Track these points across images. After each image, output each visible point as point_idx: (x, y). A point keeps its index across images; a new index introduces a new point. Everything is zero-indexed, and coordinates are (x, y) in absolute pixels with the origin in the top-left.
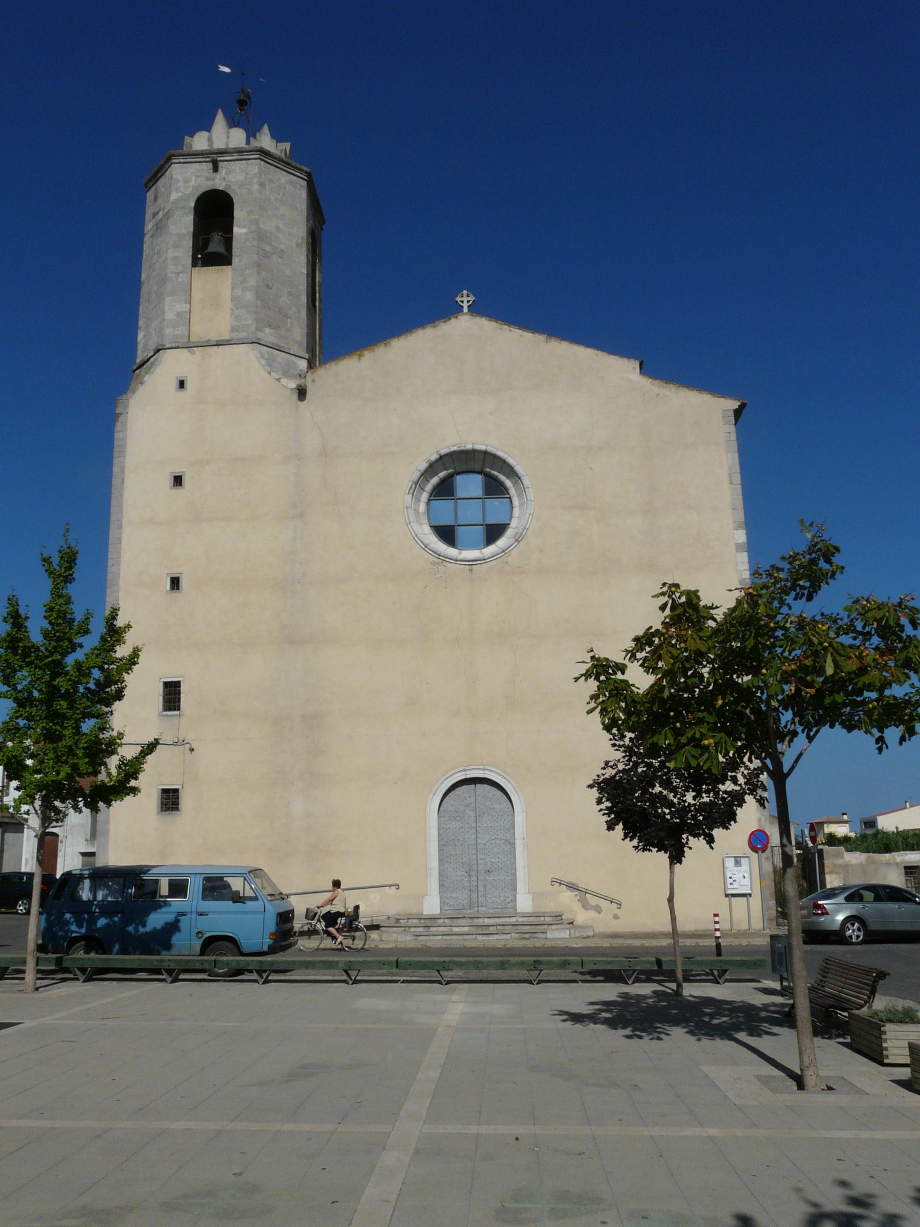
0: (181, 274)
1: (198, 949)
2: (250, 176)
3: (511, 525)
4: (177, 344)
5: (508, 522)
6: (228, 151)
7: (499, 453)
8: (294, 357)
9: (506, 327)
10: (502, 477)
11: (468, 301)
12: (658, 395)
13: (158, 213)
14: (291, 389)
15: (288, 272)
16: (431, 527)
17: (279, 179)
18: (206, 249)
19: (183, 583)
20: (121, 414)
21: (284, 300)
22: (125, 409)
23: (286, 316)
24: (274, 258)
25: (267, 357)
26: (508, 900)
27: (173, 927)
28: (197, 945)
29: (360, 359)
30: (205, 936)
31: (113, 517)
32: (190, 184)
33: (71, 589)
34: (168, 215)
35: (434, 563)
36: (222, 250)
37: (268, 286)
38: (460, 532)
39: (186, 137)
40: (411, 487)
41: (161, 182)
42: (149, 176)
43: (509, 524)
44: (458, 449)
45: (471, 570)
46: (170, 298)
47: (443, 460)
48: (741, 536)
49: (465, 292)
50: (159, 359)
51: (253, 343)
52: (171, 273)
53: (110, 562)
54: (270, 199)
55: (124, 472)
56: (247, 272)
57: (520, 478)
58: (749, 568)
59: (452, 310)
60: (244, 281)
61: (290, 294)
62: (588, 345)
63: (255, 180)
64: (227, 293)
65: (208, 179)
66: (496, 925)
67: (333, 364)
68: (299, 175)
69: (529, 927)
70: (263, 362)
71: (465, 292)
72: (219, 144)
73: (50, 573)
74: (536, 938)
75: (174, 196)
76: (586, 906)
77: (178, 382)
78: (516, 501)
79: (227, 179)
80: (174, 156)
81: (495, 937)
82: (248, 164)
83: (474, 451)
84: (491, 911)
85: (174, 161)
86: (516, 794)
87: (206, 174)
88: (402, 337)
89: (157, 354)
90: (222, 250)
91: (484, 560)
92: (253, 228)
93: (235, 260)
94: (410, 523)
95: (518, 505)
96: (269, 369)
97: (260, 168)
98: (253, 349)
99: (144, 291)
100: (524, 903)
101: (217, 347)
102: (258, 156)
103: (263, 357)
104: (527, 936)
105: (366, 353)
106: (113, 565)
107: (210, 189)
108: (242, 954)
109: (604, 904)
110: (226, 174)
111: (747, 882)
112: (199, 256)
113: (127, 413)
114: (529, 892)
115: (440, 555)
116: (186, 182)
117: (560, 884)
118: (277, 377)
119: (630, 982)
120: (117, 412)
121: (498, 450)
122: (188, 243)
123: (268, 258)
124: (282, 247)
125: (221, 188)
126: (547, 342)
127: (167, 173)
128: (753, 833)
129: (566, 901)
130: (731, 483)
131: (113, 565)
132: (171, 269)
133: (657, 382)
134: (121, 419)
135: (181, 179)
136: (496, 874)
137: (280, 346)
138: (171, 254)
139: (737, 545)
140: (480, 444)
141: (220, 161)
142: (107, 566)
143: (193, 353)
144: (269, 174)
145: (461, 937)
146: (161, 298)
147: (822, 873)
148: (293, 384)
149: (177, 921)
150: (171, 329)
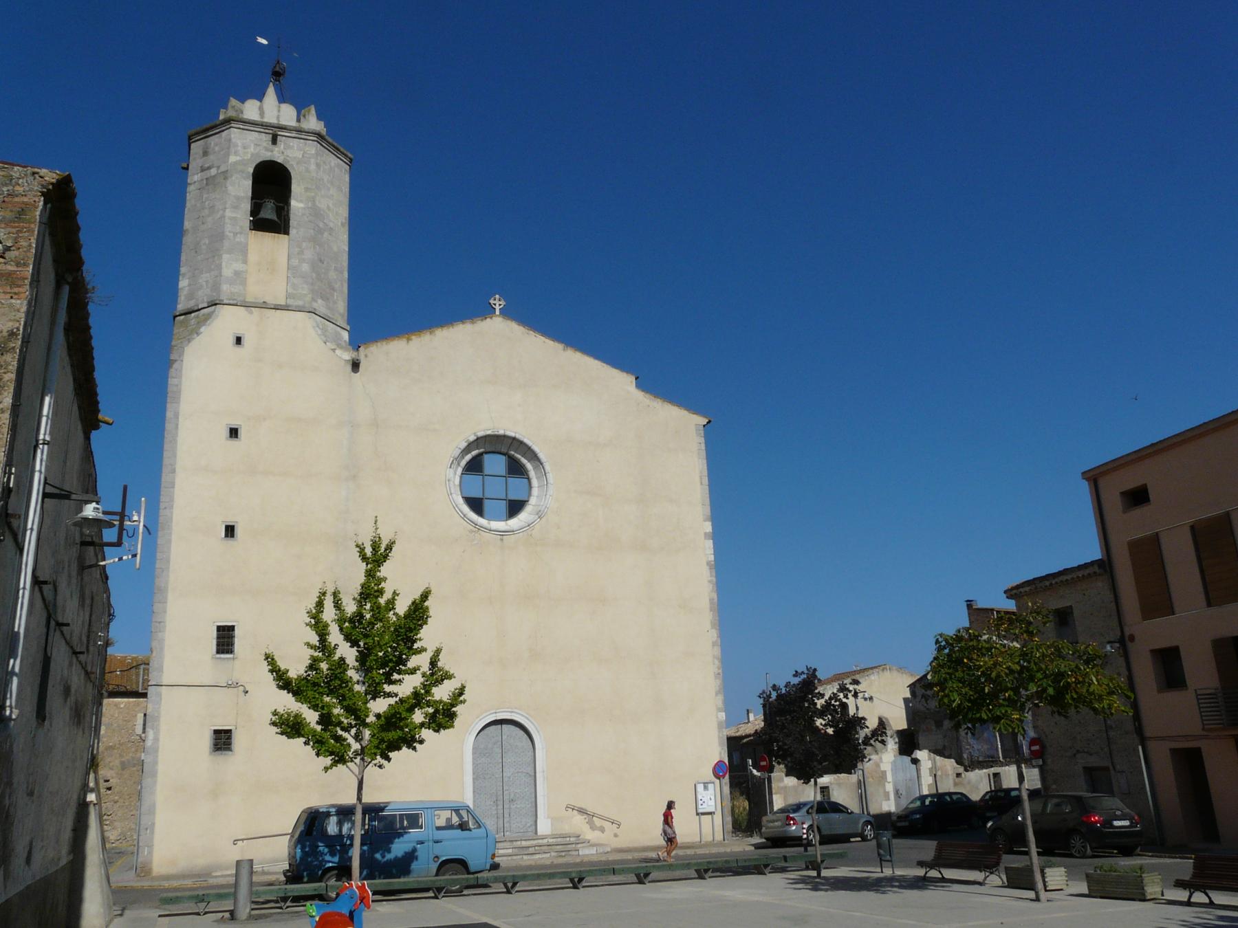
0: (239, 235)
1: (434, 871)
3: (530, 502)
4: (235, 302)
5: (526, 499)
6: (288, 128)
7: (526, 441)
8: (339, 328)
9: (531, 332)
10: (524, 461)
11: (500, 305)
12: (649, 406)
13: (209, 168)
14: (345, 360)
15: (335, 249)
16: (463, 497)
18: (258, 214)
19: (238, 531)
20: (176, 361)
21: (333, 275)
22: (180, 357)
23: (333, 289)
24: (326, 234)
25: (321, 327)
26: (529, 825)
27: (411, 856)
28: (434, 867)
29: (408, 342)
30: (440, 861)
31: (166, 461)
32: (249, 150)
33: (384, 571)
34: (225, 175)
35: (471, 531)
37: (321, 261)
38: (487, 505)
39: (231, 98)
40: (453, 461)
41: (213, 141)
42: (199, 129)
43: (528, 501)
44: (492, 433)
45: (502, 540)
46: (228, 256)
47: (479, 441)
48: (708, 527)
49: (497, 296)
50: (216, 312)
51: (309, 312)
52: (230, 232)
53: (162, 506)
54: (323, 180)
55: (178, 418)
56: (304, 245)
57: (542, 464)
58: (714, 552)
59: (486, 311)
60: (301, 253)
61: (336, 269)
62: (596, 357)
64: (283, 260)
65: (267, 149)
66: (535, 846)
67: (384, 343)
68: (345, 160)
69: (561, 847)
70: (320, 332)
71: (497, 296)
73: (364, 558)
74: (570, 855)
75: (233, 159)
76: (593, 827)
77: (235, 338)
78: (535, 482)
80: (233, 120)
81: (537, 856)
82: (306, 144)
83: (505, 436)
84: (514, 835)
85: (232, 125)
86: (537, 734)
87: (265, 144)
88: (446, 328)
89: (213, 307)
90: (274, 217)
91: (513, 531)
92: (310, 205)
93: (293, 231)
94: (451, 494)
95: (537, 486)
96: (325, 339)
98: (310, 318)
99: (188, 240)
100: (544, 827)
101: (274, 310)
102: (315, 139)
103: (318, 326)
104: (563, 854)
105: (413, 337)
106: (165, 508)
107: (269, 159)
108: (469, 873)
109: (607, 825)
110: (284, 148)
111: (712, 803)
113: (182, 361)
114: (548, 818)
115: (476, 525)
116: (245, 148)
117: (573, 809)
118: (333, 348)
119: (766, 871)
120: (172, 358)
121: (525, 437)
122: (247, 206)
123: (322, 234)
124: (331, 225)
125: (279, 161)
126: (564, 350)
127: (224, 134)
128: (717, 764)
129: (578, 824)
130: (701, 483)
131: (165, 508)
132: (228, 229)
133: (648, 396)
134: (176, 366)
135: (240, 144)
136: (519, 803)
137: (329, 317)
138: (228, 213)
139: (705, 534)
140: (511, 431)
141: (280, 135)
142: (159, 509)
143: (251, 313)
144: (323, 155)
145: (510, 858)
146: (215, 253)
147: (771, 794)
148: (347, 356)
149: (414, 850)
150: (228, 286)
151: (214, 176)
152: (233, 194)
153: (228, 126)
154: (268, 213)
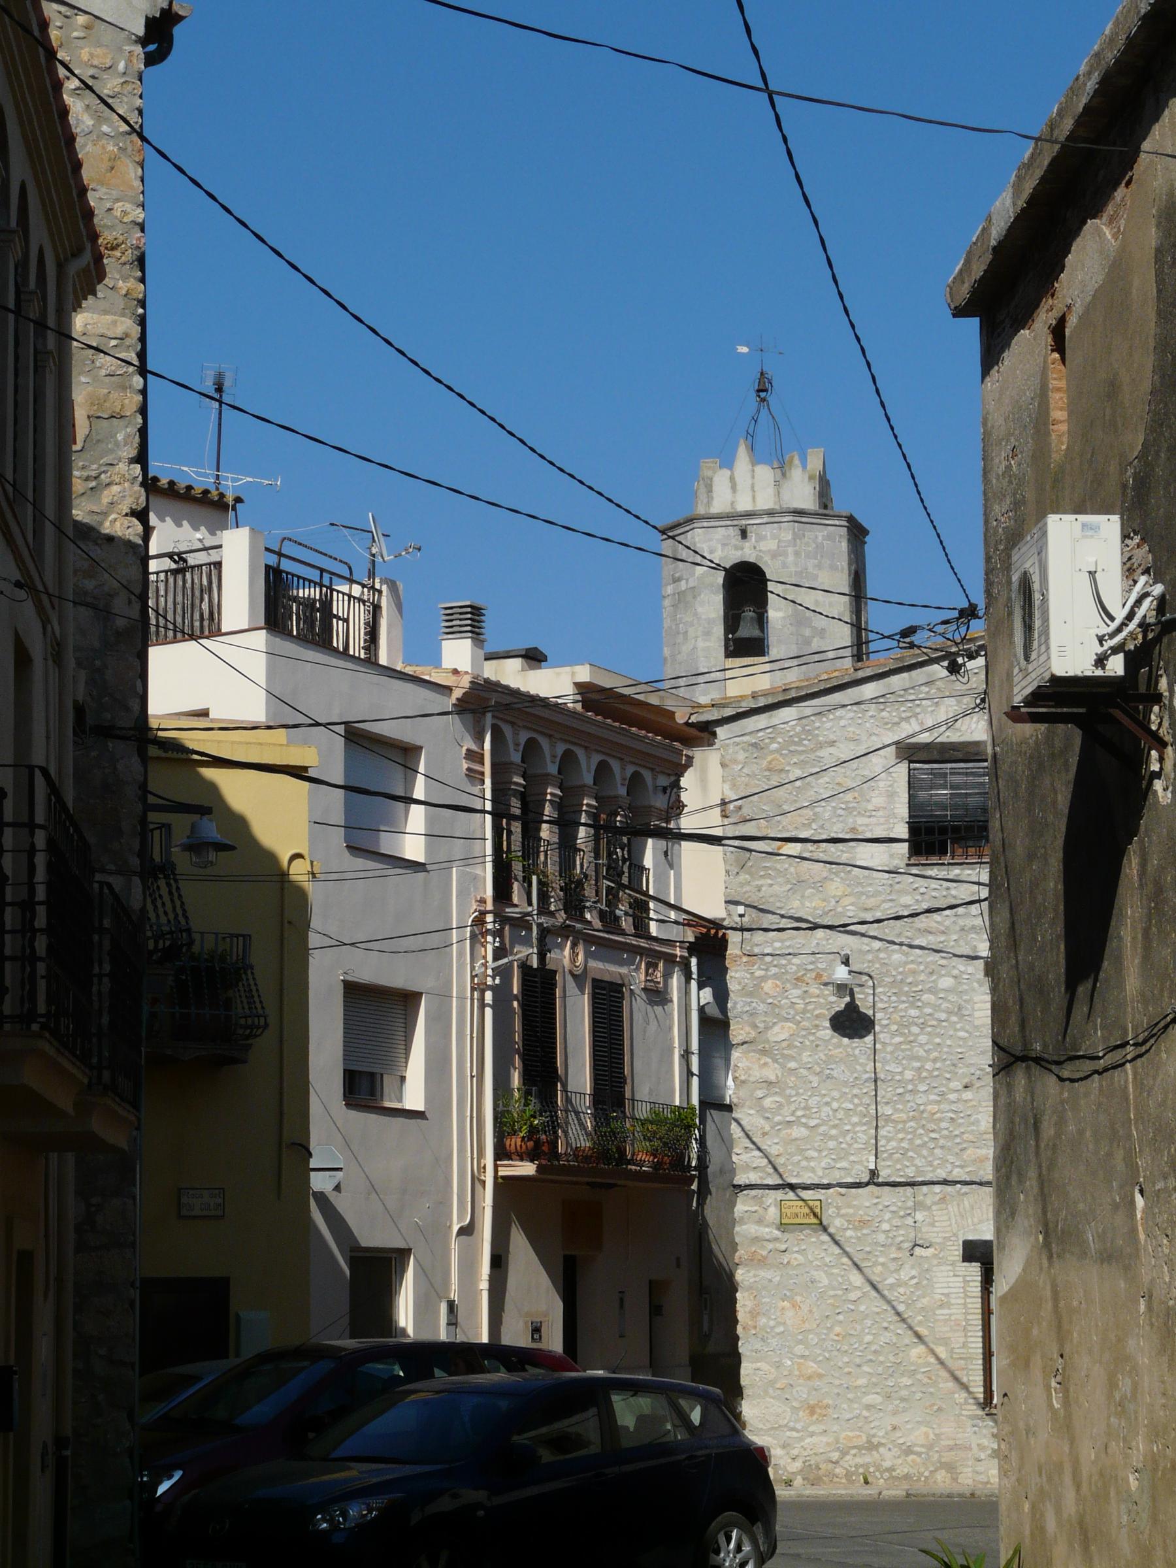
2: (783, 544)
17: (816, 537)
36: (756, 633)
63: (790, 550)
65: (736, 548)
72: (744, 505)
79: (758, 549)
85: (695, 525)
97: (794, 534)
110: (756, 541)
112: (730, 636)
122: (719, 630)
125: (751, 560)
135: (706, 548)
144: (804, 536)
151: (684, 591)
152: (703, 617)
153: (691, 527)
154: (747, 630)
